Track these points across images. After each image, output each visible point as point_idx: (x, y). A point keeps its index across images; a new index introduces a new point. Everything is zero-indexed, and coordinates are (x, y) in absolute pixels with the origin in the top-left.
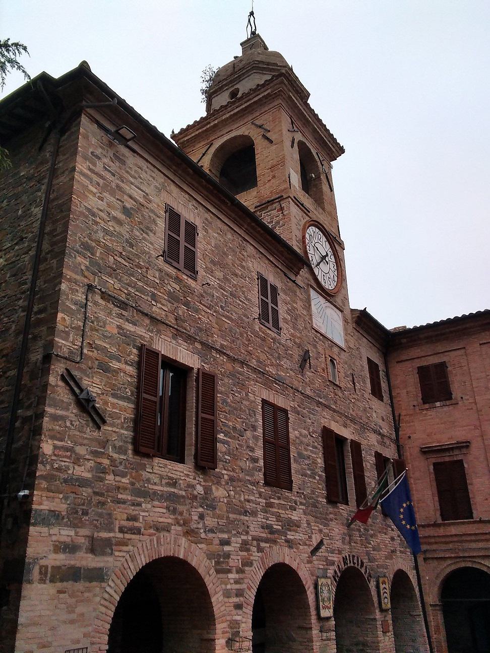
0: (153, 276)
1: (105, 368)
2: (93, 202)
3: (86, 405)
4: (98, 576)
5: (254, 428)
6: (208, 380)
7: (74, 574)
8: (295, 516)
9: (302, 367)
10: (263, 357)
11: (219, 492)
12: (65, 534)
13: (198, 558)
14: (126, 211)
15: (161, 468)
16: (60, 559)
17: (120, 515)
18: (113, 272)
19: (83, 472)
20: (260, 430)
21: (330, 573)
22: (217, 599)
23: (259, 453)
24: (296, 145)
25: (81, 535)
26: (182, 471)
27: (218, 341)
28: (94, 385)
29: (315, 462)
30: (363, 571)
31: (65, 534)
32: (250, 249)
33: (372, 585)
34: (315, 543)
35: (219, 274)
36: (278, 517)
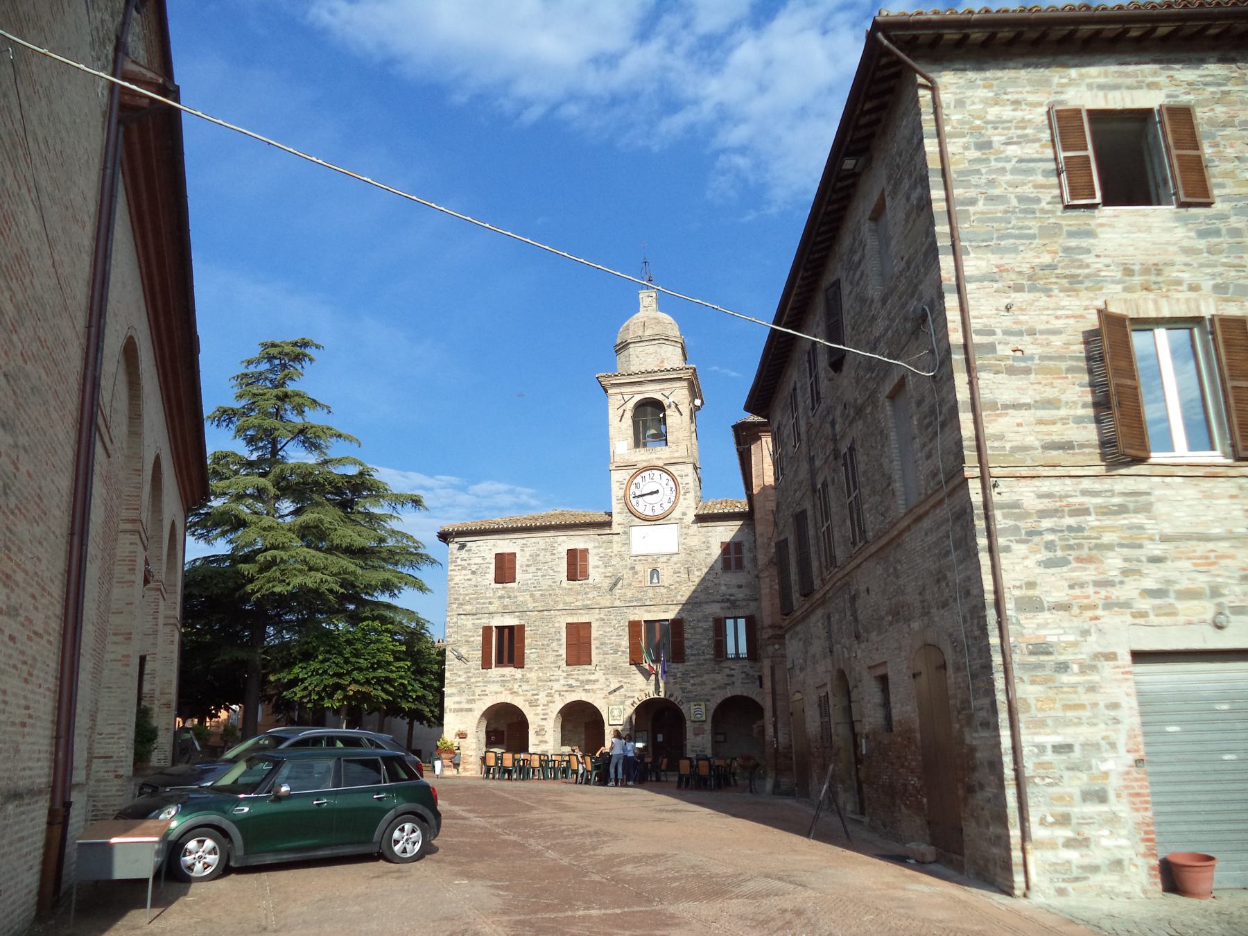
0: (489, 594)
1: (467, 641)
2: (457, 580)
3: (459, 658)
4: (470, 710)
5: (559, 640)
6: (522, 627)
7: (461, 710)
8: (593, 677)
9: (611, 590)
10: (568, 599)
11: (532, 676)
12: (457, 699)
13: (519, 702)
14: (474, 573)
15: (495, 672)
16: (457, 706)
17: (478, 691)
18: (469, 602)
19: (462, 679)
20: (564, 640)
21: (630, 701)
22: (530, 717)
23: (563, 651)
24: (629, 414)
25: (463, 698)
26: (508, 671)
27: (531, 606)
28: (463, 651)
29: (620, 645)
30: (672, 699)
31: (457, 699)
32: (561, 539)
33: (684, 708)
34: (613, 687)
35: (533, 569)
36: (577, 680)
